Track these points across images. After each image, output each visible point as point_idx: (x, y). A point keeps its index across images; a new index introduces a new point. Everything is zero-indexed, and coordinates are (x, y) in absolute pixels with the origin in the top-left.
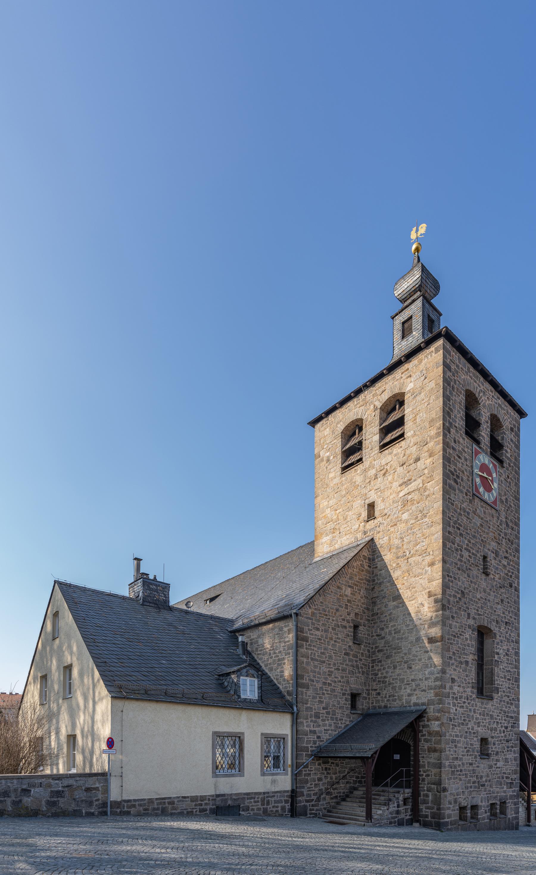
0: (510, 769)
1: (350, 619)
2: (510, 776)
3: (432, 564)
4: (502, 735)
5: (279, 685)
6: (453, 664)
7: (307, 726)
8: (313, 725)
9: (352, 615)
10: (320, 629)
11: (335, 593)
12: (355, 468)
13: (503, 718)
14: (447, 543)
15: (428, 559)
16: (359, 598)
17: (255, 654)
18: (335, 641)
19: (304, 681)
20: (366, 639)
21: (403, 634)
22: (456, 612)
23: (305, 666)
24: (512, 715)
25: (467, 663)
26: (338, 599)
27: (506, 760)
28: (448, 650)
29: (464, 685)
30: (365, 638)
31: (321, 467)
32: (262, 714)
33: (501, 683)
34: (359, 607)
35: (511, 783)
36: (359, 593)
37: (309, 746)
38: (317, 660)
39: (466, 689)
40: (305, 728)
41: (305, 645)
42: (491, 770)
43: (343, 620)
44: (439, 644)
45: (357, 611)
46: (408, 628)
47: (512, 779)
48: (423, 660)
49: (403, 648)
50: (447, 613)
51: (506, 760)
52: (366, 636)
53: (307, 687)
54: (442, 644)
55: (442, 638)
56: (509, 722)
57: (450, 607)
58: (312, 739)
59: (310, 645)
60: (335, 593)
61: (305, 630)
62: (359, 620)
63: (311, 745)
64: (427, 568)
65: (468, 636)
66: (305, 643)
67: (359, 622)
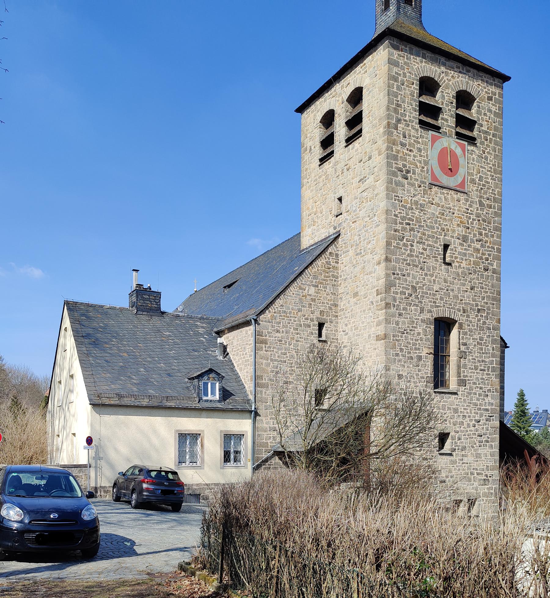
0: (484, 465)
1: (314, 317)
2: (483, 472)
3: (379, 263)
4: (473, 428)
5: (245, 384)
6: (400, 361)
7: (266, 423)
8: (273, 422)
9: (317, 314)
10: (281, 330)
11: (296, 294)
12: (329, 161)
13: (473, 411)
14: (393, 241)
15: (377, 258)
16: (325, 295)
17: (231, 354)
18: (297, 341)
19: (264, 381)
20: (334, 335)
21: (360, 331)
22: (404, 309)
23: (264, 367)
24: (487, 408)
25: (420, 358)
26: (300, 299)
27: (478, 456)
28: (394, 347)
29: (415, 380)
30: (332, 334)
31: (306, 157)
32: (221, 413)
33: (469, 375)
34: (325, 305)
35: (484, 479)
36: (325, 291)
37: (269, 441)
38: (276, 360)
39: (418, 384)
40: (265, 425)
41: (264, 347)
42: (455, 465)
43: (307, 319)
44: (383, 341)
45: (322, 309)
46: (363, 325)
47: (486, 476)
48: (373, 358)
49: (360, 345)
50: (393, 310)
51: (478, 456)
52: (333, 332)
53: (266, 386)
54: (385, 342)
55: (385, 336)
56: (481, 415)
57: (396, 304)
58: (272, 435)
59: (269, 347)
60: (296, 294)
61: (265, 332)
62: (325, 317)
63: (271, 441)
64: (376, 267)
65: (421, 331)
66: (264, 345)
67: (324, 319)
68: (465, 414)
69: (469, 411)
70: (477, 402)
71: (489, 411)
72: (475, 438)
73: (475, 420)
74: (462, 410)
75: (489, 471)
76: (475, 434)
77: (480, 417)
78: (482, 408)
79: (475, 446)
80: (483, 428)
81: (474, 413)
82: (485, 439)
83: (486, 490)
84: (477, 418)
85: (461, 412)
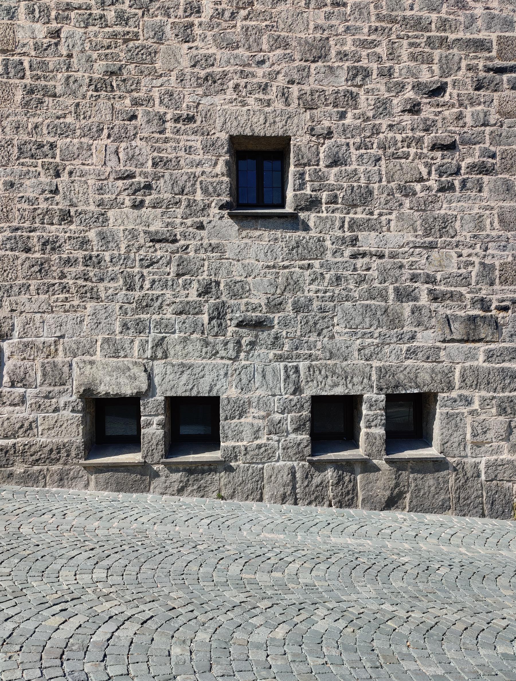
13: (404, 52)
68: (364, 63)
69: (382, 50)
70: (425, 14)
71: (489, 50)
72: (419, 156)
73: (417, 87)
74: (348, 47)
75: (497, 287)
76: (419, 141)
77: (445, 73)
78: (452, 37)
79: (418, 187)
80: (459, 117)
81: (413, 57)
82: (469, 160)
83: (480, 361)
84: (425, 77)
85: (343, 56)
